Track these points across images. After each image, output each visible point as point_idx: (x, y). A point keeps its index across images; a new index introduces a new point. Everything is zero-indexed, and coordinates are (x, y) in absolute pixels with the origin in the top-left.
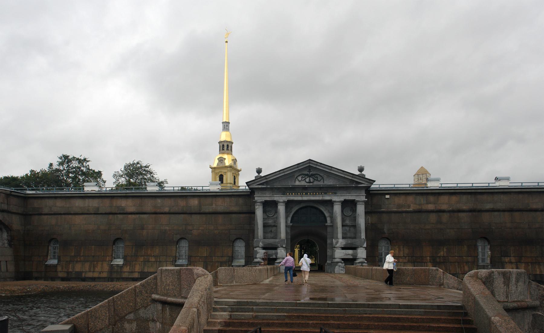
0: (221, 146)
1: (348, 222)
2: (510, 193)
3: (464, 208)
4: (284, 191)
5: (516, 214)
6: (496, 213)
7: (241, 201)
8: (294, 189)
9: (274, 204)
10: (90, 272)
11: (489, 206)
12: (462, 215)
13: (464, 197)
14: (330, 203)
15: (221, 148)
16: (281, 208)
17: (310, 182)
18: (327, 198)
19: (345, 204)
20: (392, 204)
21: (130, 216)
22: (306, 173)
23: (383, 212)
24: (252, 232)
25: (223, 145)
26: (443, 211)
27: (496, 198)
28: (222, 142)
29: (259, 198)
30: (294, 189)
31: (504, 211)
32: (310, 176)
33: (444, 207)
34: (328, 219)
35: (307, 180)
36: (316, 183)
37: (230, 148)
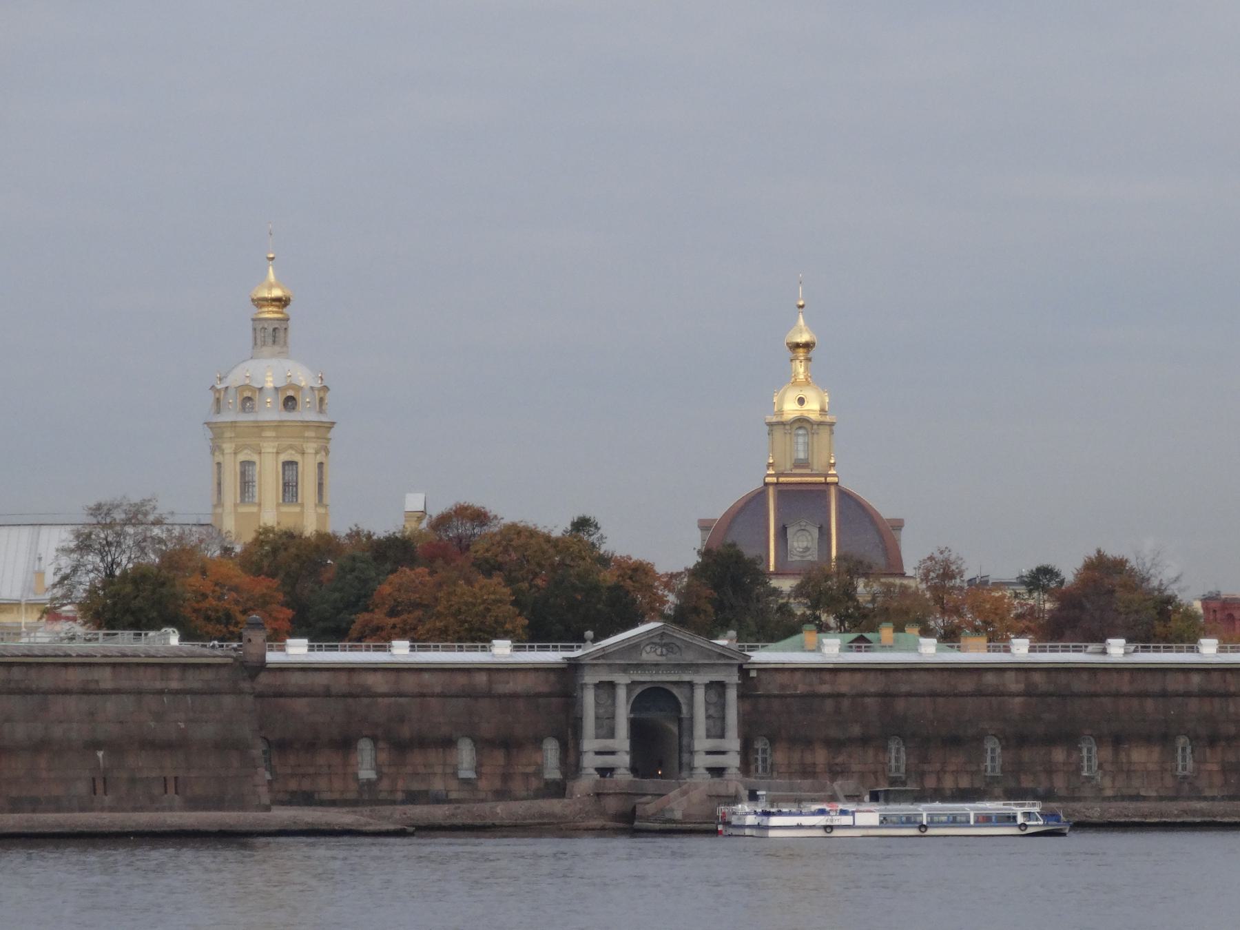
1: (711, 712)
2: (933, 670)
3: (872, 690)
4: (625, 668)
5: (940, 700)
6: (914, 699)
7: (552, 677)
8: (639, 666)
9: (612, 685)
11: (904, 688)
12: (868, 700)
13: (872, 676)
14: (691, 684)
16: (622, 693)
17: (662, 655)
18: (686, 678)
19: (710, 686)
20: (771, 686)
21: (380, 700)
22: (657, 640)
23: (760, 696)
24: (576, 726)
26: (843, 695)
27: (915, 676)
29: (590, 678)
30: (639, 666)
31: (923, 696)
32: (662, 646)
33: (844, 689)
34: (684, 709)
35: (659, 652)
36: (671, 656)
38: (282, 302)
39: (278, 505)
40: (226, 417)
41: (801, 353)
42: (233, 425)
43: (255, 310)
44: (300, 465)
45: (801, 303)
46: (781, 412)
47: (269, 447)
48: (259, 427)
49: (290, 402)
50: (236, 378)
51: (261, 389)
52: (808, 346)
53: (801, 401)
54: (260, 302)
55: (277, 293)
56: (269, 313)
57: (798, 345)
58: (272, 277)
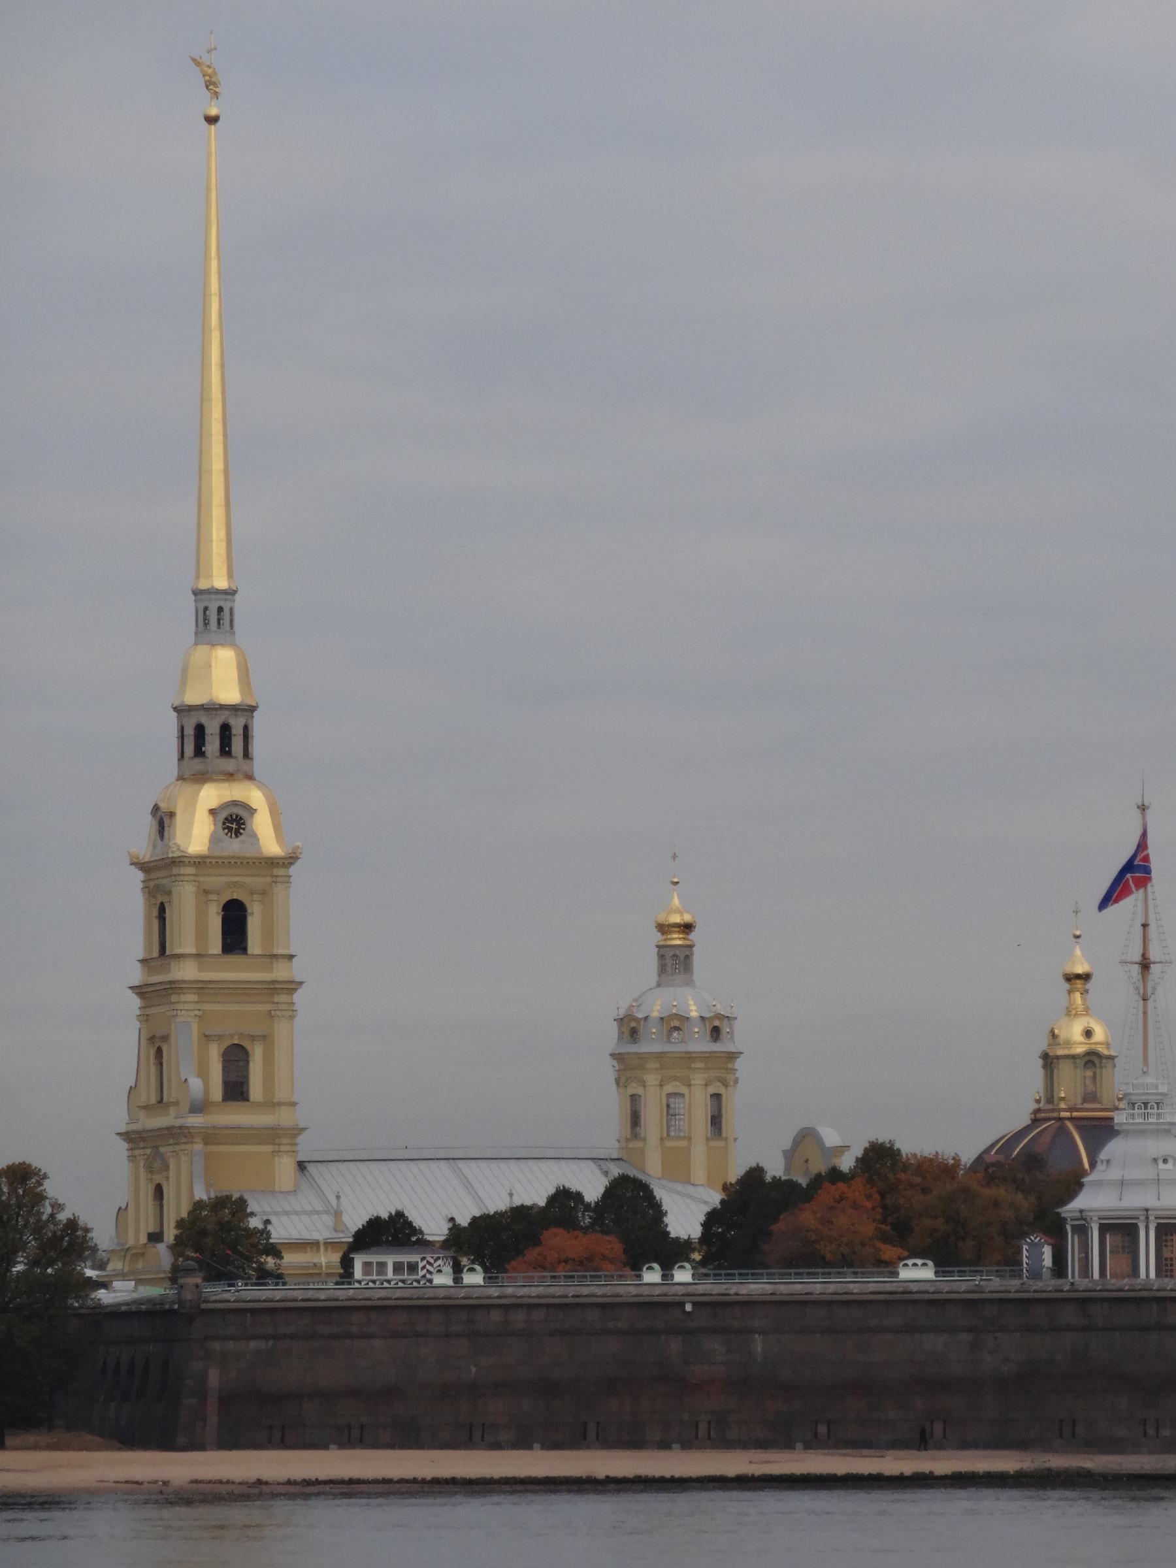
0: (190, 731)
10: (362, 1426)
15: (190, 749)
25: (200, 730)
28: (191, 709)
37: (237, 745)
38: (687, 928)
39: (707, 1139)
40: (644, 1047)
41: (1079, 984)
42: (660, 1056)
43: (659, 936)
44: (724, 1098)
45: (1078, 933)
46: (1068, 1044)
47: (698, 1079)
48: (689, 1057)
49: (716, 1033)
50: (656, 1007)
51: (646, 1018)
52: (1086, 977)
53: (1088, 1033)
54: (663, 928)
55: (687, 918)
56: (676, 940)
57: (1078, 977)
58: (676, 901)
